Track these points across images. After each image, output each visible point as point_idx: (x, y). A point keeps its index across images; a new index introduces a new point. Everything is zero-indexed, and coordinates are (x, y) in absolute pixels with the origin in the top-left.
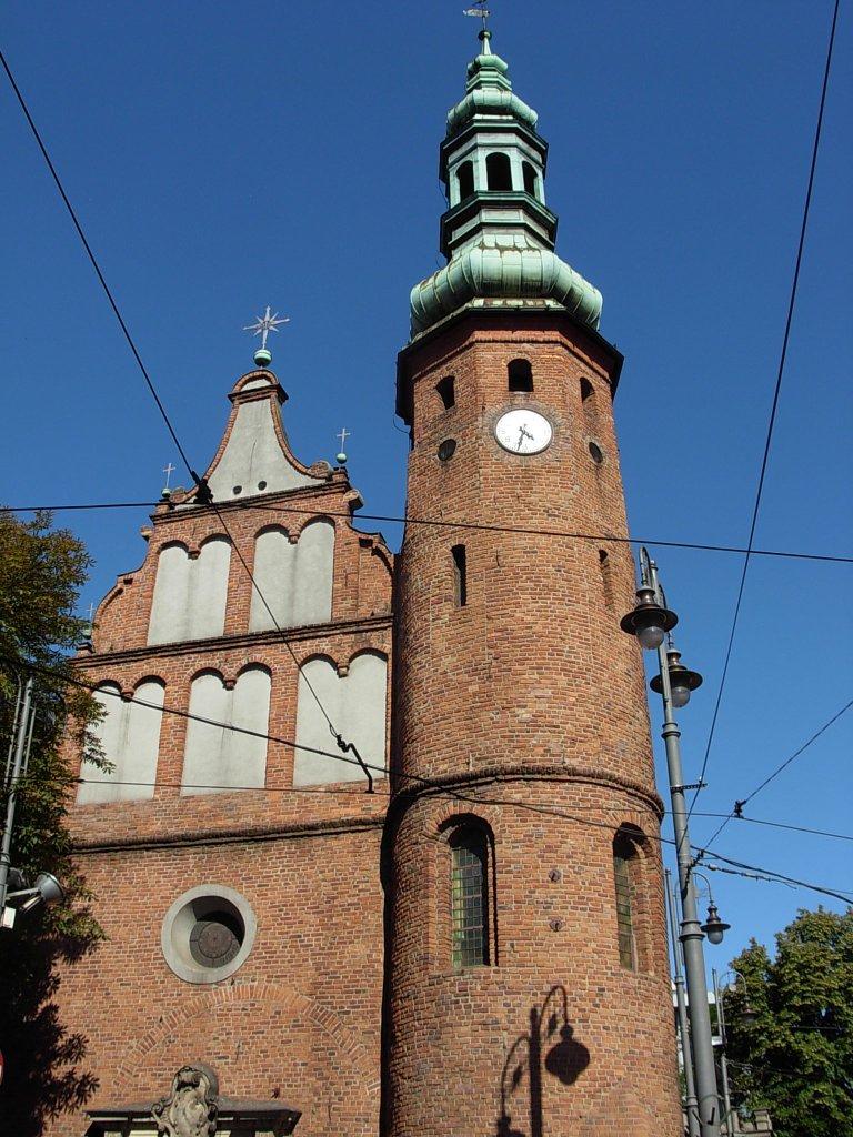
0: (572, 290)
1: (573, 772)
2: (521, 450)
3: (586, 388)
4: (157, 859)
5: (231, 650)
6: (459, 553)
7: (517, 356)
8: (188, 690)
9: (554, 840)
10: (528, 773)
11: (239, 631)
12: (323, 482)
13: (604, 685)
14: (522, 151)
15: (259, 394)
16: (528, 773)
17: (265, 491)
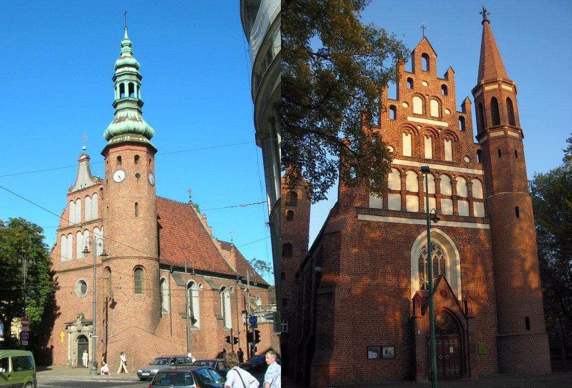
0: (135, 129)
1: (124, 257)
2: (122, 179)
3: (137, 158)
4: (73, 273)
5: (83, 226)
6: (108, 207)
7: (118, 155)
8: (76, 236)
9: (120, 271)
10: (116, 258)
11: (83, 222)
12: (95, 184)
13: (134, 236)
14: (128, 80)
15: (83, 160)
16: (116, 258)
17: (86, 187)
